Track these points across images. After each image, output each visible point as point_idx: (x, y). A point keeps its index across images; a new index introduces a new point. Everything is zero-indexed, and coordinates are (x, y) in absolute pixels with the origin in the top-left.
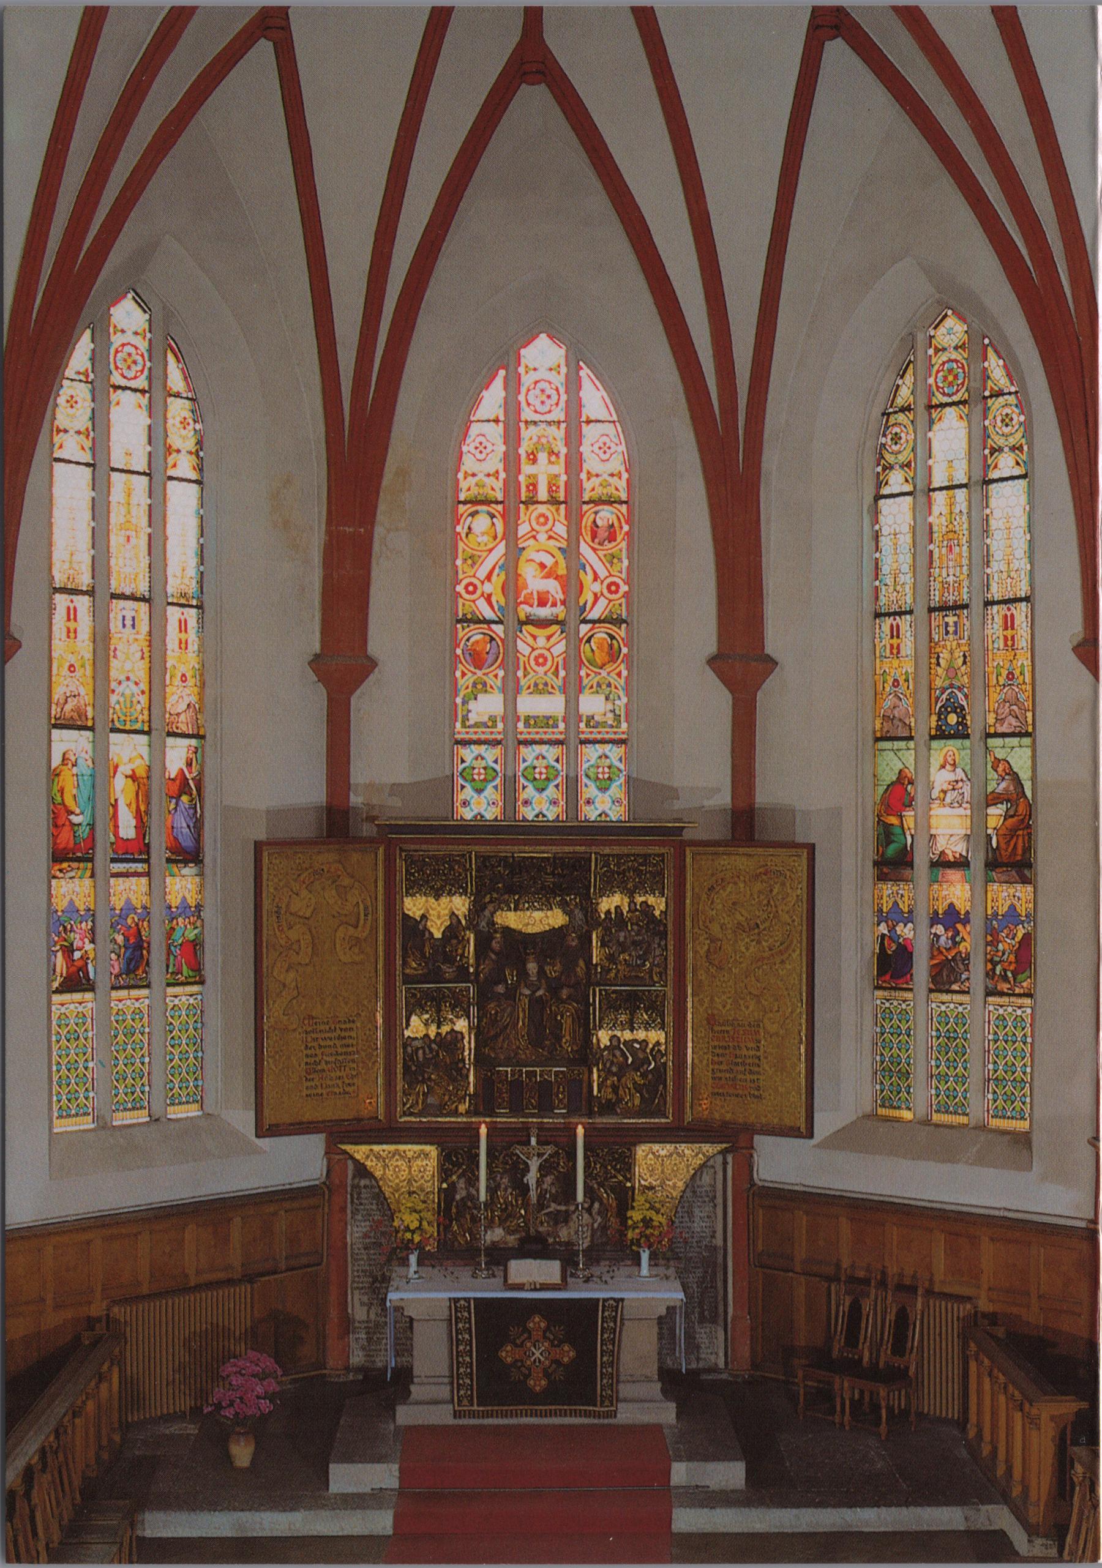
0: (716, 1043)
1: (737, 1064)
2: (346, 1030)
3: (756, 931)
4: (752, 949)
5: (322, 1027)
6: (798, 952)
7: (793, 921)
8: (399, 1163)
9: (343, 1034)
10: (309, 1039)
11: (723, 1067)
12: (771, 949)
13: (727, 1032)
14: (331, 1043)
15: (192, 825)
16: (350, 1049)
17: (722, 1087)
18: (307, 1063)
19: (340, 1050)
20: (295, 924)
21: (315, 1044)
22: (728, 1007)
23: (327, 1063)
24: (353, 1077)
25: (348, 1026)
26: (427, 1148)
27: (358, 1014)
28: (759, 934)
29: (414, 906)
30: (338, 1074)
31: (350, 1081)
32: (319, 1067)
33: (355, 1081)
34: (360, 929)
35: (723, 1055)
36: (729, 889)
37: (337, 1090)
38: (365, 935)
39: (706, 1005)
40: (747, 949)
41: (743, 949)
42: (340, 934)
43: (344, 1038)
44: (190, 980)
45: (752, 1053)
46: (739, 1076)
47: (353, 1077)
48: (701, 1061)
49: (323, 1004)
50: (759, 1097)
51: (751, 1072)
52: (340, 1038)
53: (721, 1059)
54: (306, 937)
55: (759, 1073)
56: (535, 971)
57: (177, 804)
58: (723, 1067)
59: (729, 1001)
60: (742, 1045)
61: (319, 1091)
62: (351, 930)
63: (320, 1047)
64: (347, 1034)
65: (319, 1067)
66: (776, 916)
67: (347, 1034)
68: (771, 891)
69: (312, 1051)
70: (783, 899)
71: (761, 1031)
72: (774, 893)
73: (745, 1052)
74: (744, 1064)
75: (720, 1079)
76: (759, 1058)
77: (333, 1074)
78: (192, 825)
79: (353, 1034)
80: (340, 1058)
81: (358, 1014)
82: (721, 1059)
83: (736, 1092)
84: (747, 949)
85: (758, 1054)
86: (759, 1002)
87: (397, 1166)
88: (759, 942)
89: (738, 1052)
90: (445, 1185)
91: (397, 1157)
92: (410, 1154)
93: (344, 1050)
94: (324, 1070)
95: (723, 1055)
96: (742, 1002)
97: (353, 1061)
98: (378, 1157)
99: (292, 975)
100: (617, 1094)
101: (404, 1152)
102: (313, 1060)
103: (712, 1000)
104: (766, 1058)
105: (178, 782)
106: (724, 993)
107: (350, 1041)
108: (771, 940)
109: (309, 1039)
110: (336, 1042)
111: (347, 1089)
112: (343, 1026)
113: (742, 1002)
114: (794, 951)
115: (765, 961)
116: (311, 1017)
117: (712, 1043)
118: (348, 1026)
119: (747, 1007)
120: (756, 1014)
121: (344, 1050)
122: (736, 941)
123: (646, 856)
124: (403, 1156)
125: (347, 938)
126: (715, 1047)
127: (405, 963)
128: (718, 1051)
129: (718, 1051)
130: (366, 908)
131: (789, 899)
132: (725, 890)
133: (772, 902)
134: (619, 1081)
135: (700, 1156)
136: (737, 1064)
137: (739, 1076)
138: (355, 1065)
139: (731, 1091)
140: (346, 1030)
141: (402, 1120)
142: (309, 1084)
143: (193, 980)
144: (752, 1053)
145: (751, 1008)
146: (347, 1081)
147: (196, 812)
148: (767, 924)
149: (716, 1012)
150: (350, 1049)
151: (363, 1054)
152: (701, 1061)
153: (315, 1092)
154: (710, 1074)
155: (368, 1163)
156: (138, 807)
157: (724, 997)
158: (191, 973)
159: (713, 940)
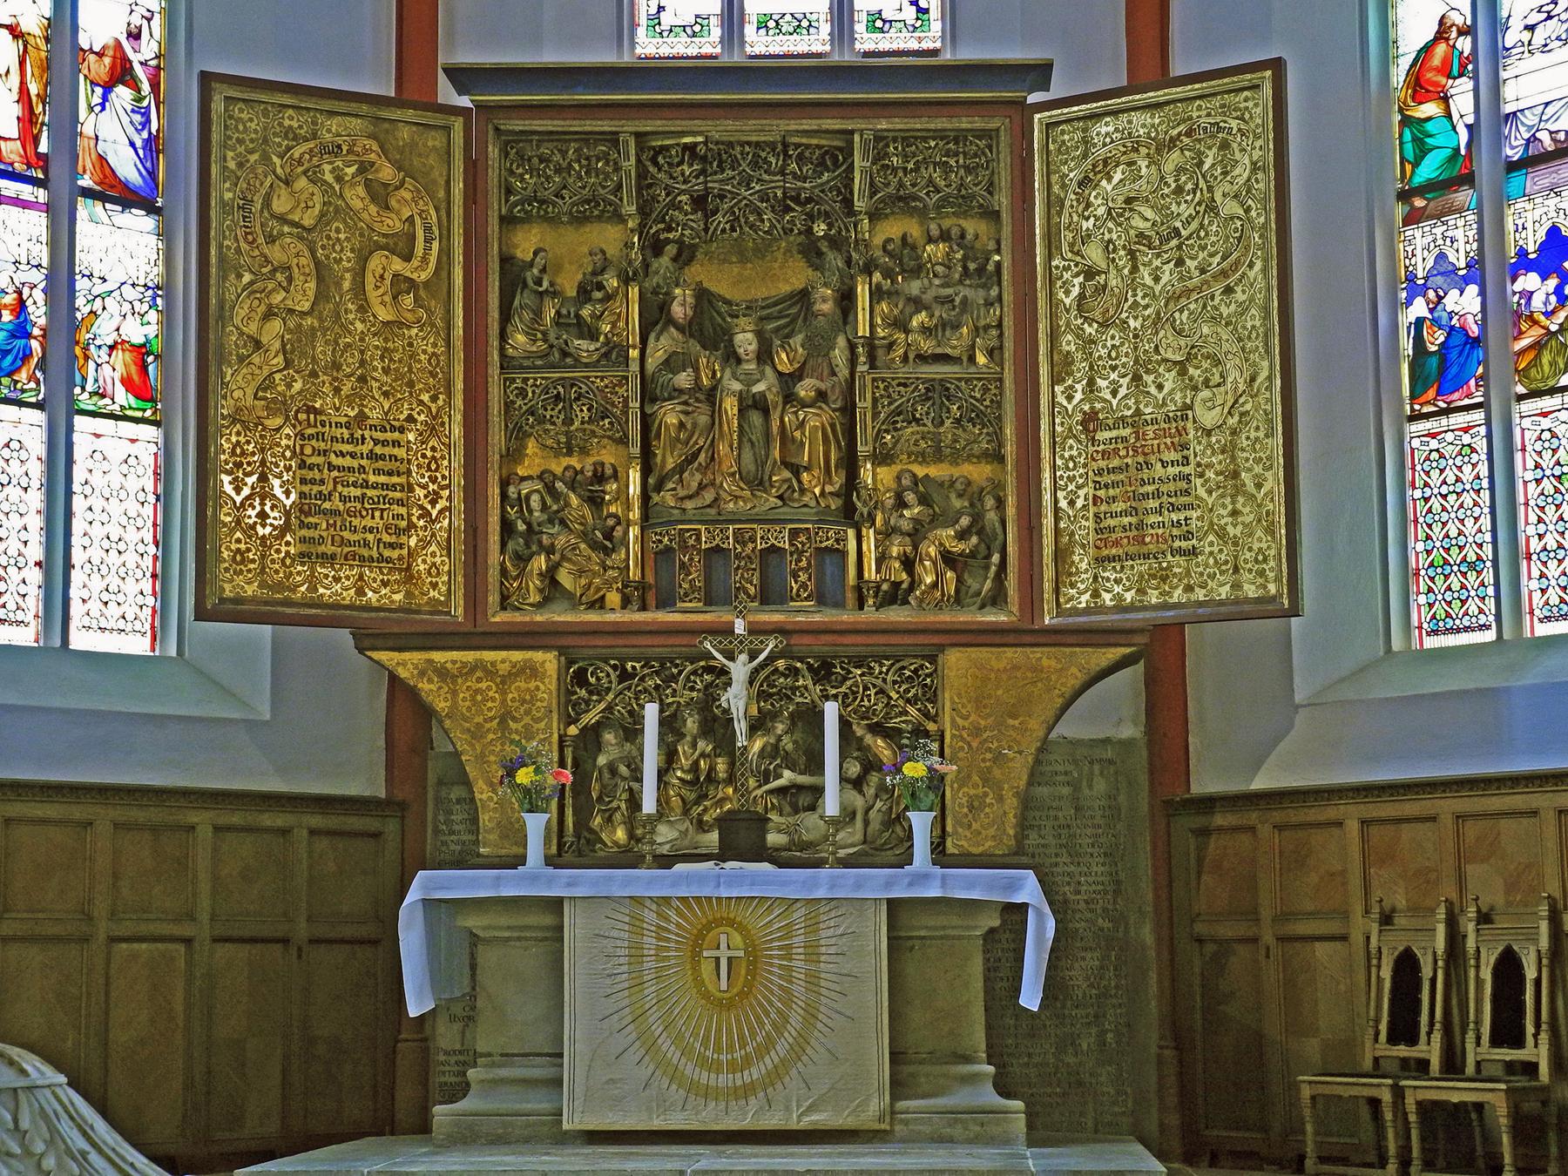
0: (1102, 464)
1: (1146, 496)
2: (385, 443)
3: (1174, 242)
4: (1165, 278)
5: (338, 432)
6: (1258, 265)
7: (1247, 211)
8: (483, 685)
9: (378, 450)
10: (308, 451)
11: (1119, 506)
12: (1203, 271)
13: (1124, 439)
14: (355, 464)
15: (139, 144)
16: (395, 479)
17: (1117, 543)
18: (302, 495)
19: (372, 479)
20: (282, 234)
21: (320, 460)
22: (1122, 392)
23: (344, 499)
24: (399, 532)
25: (389, 436)
26: (538, 656)
27: (410, 419)
28: (1179, 247)
29: (526, 242)
30: (368, 522)
31: (393, 539)
32: (327, 505)
33: (403, 539)
34: (415, 263)
35: (1114, 485)
36: (1117, 177)
37: (365, 552)
38: (424, 276)
39: (1078, 396)
40: (1157, 279)
41: (1149, 281)
42: (376, 263)
43: (382, 457)
44: (129, 413)
45: (1171, 471)
46: (1153, 519)
47: (399, 532)
48: (1072, 503)
49: (337, 390)
50: (1193, 552)
51: (1173, 508)
52: (372, 456)
53: (1111, 492)
54: (303, 261)
55: (1190, 507)
56: (753, 347)
57: (105, 98)
58: (1119, 506)
59: (1125, 381)
60: (1152, 459)
61: (329, 549)
62: (397, 265)
63: (331, 467)
64: (388, 451)
65: (327, 505)
66: (1212, 208)
67: (388, 451)
68: (1200, 164)
69: (316, 474)
70: (1225, 173)
71: (1190, 425)
72: (1206, 167)
73: (1159, 470)
74: (1157, 494)
75: (1112, 530)
76: (1187, 478)
77: (356, 522)
78: (139, 144)
79: (401, 453)
80: (370, 493)
81: (410, 419)
82: (1111, 492)
83: (1145, 550)
84: (1157, 279)
85: (1187, 470)
86: (1183, 372)
87: (477, 691)
88: (1180, 262)
89: (1145, 474)
90: (573, 730)
91: (479, 674)
92: (504, 669)
93: (382, 479)
94: (336, 513)
95: (1114, 485)
96: (1149, 379)
97: (400, 502)
98: (442, 673)
99: (276, 325)
100: (911, 573)
101: (493, 664)
102: (316, 488)
103: (1091, 382)
104: (1201, 475)
105: (107, 61)
106: (1114, 368)
107: (394, 465)
108: (1201, 255)
109: (308, 451)
110: (364, 462)
111: (387, 553)
112: (379, 435)
113: (1149, 379)
114: (1251, 266)
115: (1195, 296)
116: (311, 410)
117: (1095, 465)
118: (389, 436)
119: (1160, 387)
120: (1178, 396)
121: (382, 479)
122: (1135, 269)
123: (959, 137)
124: (489, 671)
125: (388, 277)
126: (1100, 472)
127: (503, 337)
128: (1106, 479)
129: (1106, 479)
130: (428, 229)
131: (1237, 172)
132: (1109, 179)
133: (1202, 184)
134: (916, 547)
135: (1074, 670)
136: (1146, 496)
137: (1153, 519)
138: (403, 511)
139: (1132, 549)
140: (385, 443)
141: (497, 619)
142: (304, 532)
143: (139, 414)
144: (1171, 471)
145: (1168, 386)
146: (386, 538)
147: (148, 121)
148: (1195, 225)
149: (1098, 406)
150: (395, 479)
151: (420, 492)
152: (1072, 503)
153: (322, 549)
154: (1091, 524)
155: (424, 686)
156: (23, 83)
157: (1113, 376)
158: (133, 401)
159: (1090, 273)
